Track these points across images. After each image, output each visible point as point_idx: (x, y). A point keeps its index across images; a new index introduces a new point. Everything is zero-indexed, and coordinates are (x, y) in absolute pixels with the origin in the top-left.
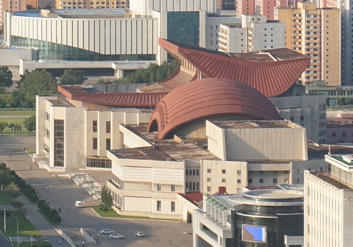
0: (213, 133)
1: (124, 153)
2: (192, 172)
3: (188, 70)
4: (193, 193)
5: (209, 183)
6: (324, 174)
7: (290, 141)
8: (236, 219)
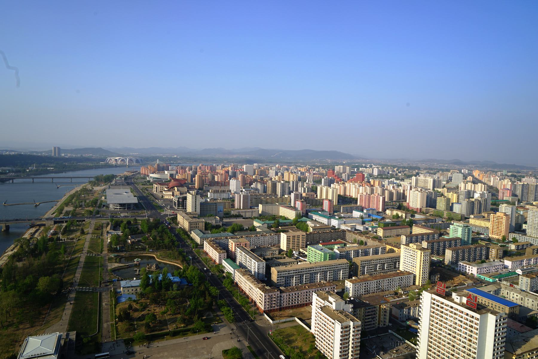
0: (176, 188)
1: (165, 191)
2: (173, 193)
3: (172, 181)
4: (173, 195)
5: (175, 194)
6: (189, 193)
7: (185, 189)
8: (179, 199)
